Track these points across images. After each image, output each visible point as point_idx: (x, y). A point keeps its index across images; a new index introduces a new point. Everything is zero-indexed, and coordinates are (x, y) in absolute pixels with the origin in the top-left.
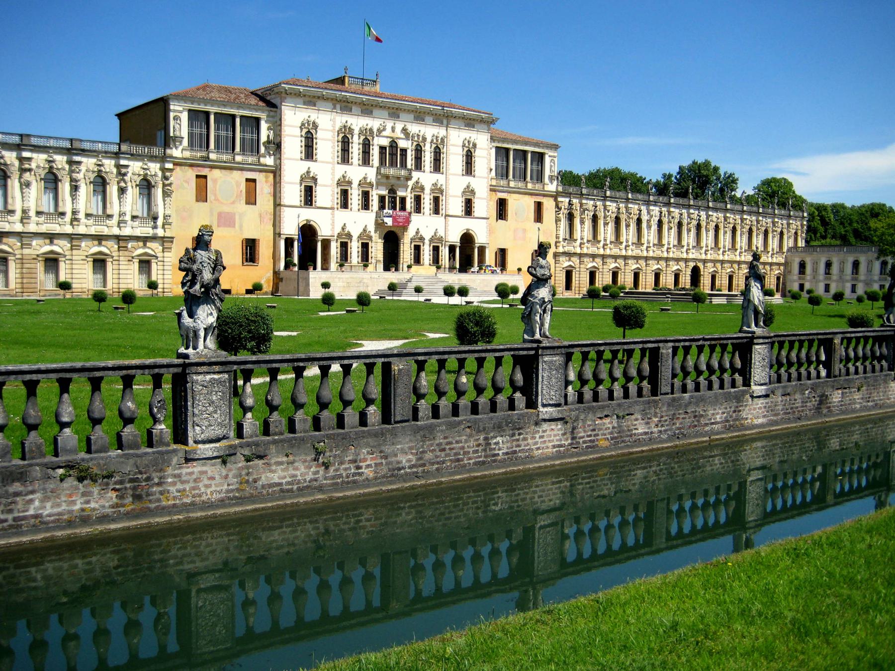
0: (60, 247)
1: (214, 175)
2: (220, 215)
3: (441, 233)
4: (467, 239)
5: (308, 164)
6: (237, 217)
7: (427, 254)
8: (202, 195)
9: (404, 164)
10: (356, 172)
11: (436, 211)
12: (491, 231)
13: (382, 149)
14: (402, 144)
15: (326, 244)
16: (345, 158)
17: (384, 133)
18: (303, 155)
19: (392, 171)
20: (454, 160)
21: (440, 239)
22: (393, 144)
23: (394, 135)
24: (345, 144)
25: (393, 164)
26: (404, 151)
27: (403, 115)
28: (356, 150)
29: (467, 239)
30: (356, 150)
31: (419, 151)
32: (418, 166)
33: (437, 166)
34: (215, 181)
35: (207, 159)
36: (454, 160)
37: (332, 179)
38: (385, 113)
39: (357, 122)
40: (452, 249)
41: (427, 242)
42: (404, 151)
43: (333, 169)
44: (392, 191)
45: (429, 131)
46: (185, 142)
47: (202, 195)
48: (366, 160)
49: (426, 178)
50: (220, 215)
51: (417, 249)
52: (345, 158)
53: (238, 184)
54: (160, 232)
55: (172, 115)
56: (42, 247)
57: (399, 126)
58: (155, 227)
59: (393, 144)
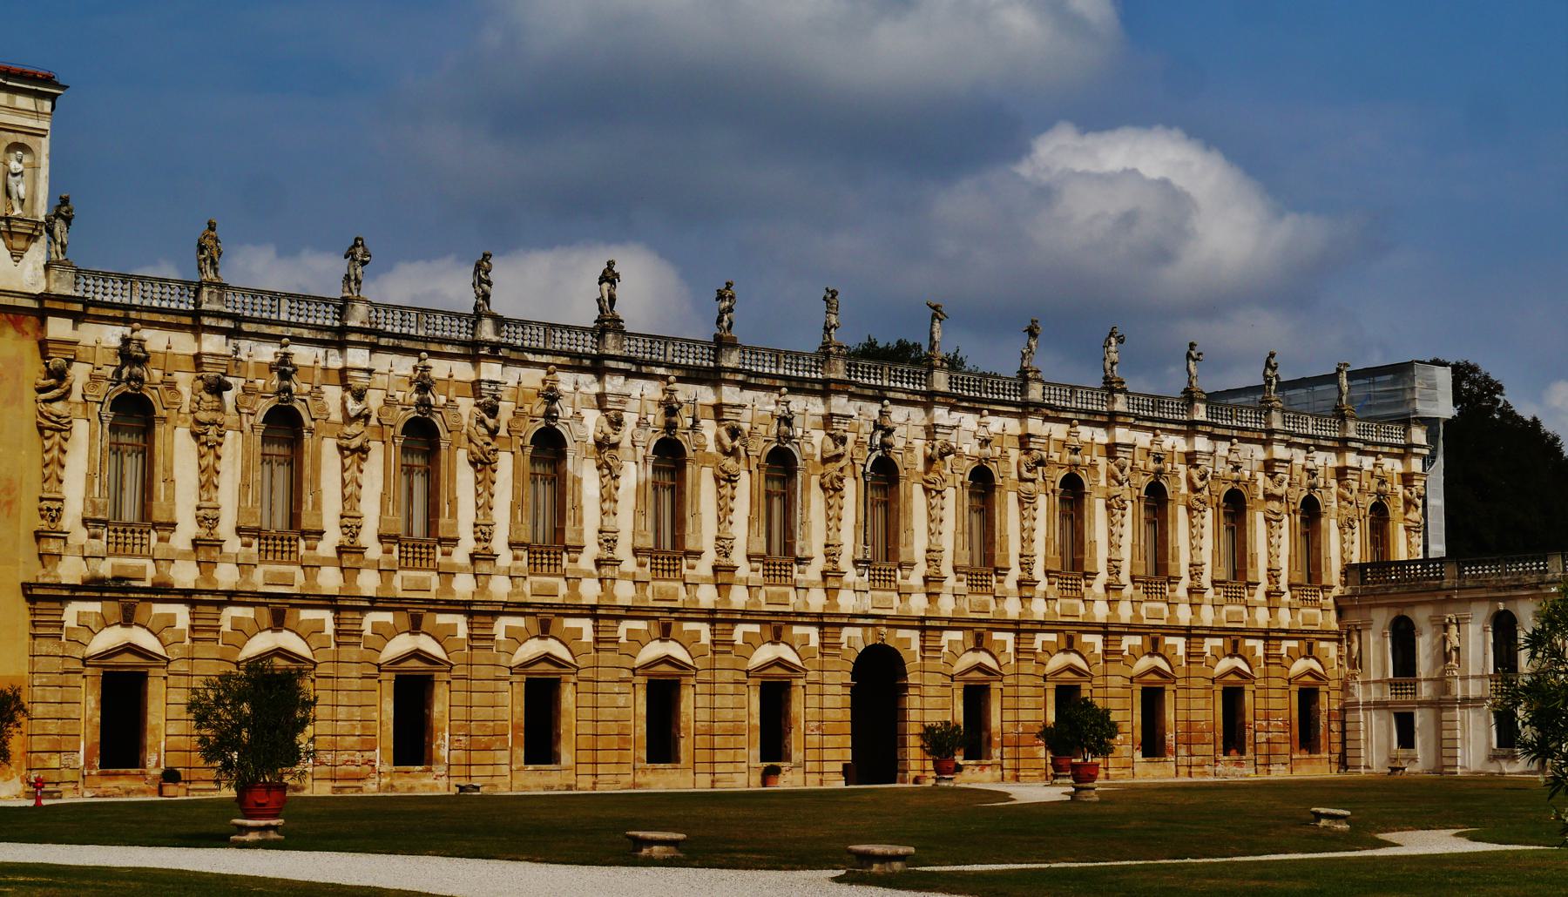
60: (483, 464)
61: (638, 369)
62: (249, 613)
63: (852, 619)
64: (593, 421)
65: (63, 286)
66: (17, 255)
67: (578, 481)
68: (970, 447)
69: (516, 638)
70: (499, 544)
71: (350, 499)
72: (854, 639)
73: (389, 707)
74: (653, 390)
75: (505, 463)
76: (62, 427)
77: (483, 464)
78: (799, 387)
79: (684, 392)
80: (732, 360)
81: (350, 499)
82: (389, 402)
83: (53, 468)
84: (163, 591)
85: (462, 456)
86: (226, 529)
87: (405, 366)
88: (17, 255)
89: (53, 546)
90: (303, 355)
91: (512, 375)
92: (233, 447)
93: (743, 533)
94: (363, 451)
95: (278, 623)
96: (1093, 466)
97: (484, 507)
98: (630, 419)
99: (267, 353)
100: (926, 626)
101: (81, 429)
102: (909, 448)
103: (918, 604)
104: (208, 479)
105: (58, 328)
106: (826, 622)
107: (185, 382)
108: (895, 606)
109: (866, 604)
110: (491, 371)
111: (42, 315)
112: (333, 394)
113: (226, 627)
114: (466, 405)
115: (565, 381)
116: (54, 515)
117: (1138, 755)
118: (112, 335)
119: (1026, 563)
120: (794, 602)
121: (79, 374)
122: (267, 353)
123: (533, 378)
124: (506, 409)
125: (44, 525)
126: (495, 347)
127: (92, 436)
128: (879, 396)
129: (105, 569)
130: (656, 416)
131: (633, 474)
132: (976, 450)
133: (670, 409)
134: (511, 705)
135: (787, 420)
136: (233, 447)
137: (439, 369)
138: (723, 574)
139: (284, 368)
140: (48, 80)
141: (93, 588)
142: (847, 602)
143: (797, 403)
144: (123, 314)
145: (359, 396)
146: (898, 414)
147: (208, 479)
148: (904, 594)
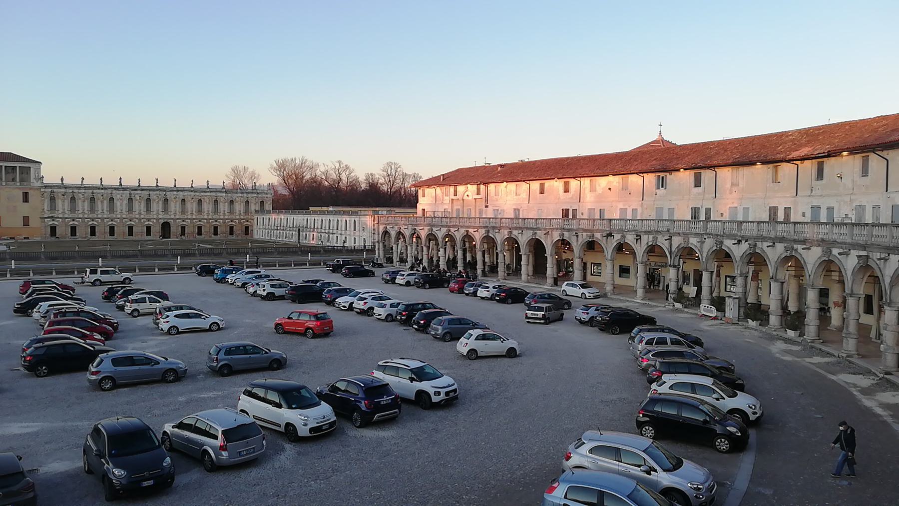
60: (102, 202)
62: (69, 220)
66: (37, 182)
67: (116, 203)
68: (182, 197)
69: (108, 222)
71: (83, 206)
72: (162, 221)
73: (89, 230)
75: (105, 201)
76: (44, 200)
77: (102, 202)
79: (132, 192)
81: (83, 206)
83: (43, 204)
84: (58, 218)
87: (91, 191)
88: (37, 182)
89: (43, 213)
90: (75, 191)
91: (106, 191)
92: (66, 201)
93: (161, 209)
97: (102, 207)
100: (175, 220)
101: (46, 200)
102: (171, 197)
103: (173, 217)
104: (63, 205)
105: (42, 190)
106: (157, 219)
108: (169, 217)
109: (164, 217)
110: (103, 191)
113: (66, 221)
118: (50, 190)
119: (208, 211)
120: (152, 217)
121: (45, 194)
122: (71, 191)
124: (105, 195)
125: (42, 211)
127: (48, 201)
129: (50, 215)
130: (128, 195)
131: (126, 202)
133: (130, 194)
134: (108, 229)
135: (149, 195)
136: (66, 201)
137: (95, 191)
138: (224, 214)
140: (40, 162)
141: (48, 217)
142: (160, 216)
143: (151, 192)
145: (83, 195)
146: (168, 193)
148: (170, 215)
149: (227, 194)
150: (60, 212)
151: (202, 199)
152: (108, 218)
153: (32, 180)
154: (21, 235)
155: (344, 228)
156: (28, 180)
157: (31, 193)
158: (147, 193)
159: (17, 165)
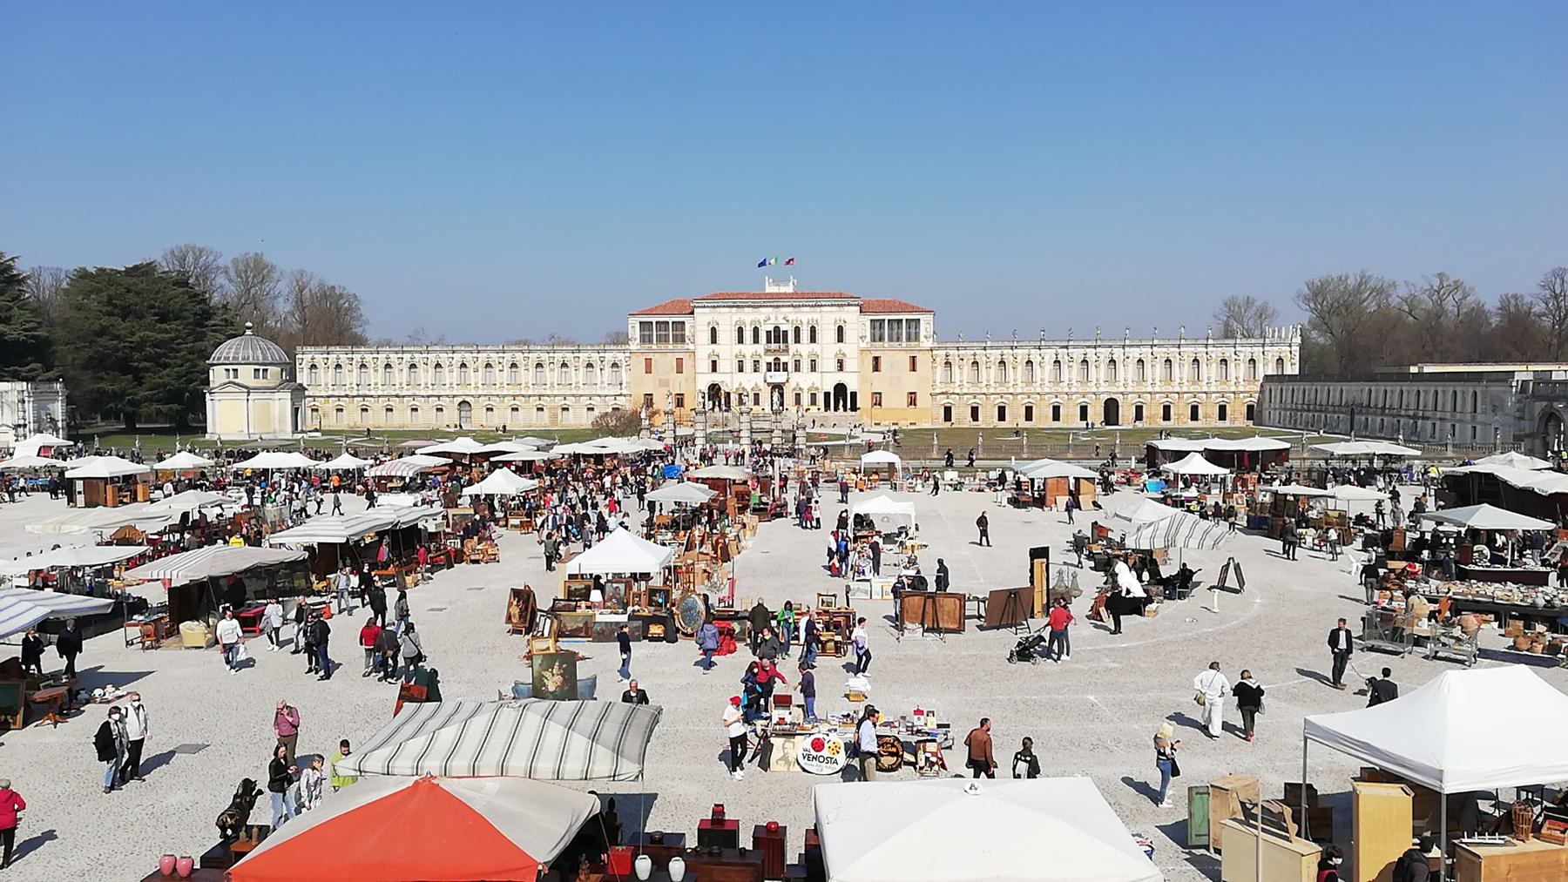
0: (570, 402)
1: (655, 358)
2: (660, 380)
3: (818, 384)
4: (840, 389)
5: (714, 346)
6: (671, 382)
7: (806, 399)
8: (648, 371)
9: (786, 341)
10: (749, 348)
11: (813, 369)
12: (863, 380)
13: (768, 333)
14: (783, 328)
15: (728, 395)
16: (741, 340)
17: (769, 322)
18: (710, 342)
19: (773, 346)
20: (827, 334)
21: (817, 389)
22: (777, 329)
23: (777, 322)
24: (740, 331)
25: (777, 341)
26: (785, 332)
27: (783, 309)
28: (748, 335)
29: (840, 389)
30: (748, 335)
31: (797, 330)
32: (797, 340)
33: (813, 339)
34: (656, 361)
35: (650, 348)
36: (827, 334)
37: (731, 355)
38: (771, 309)
39: (748, 317)
40: (827, 395)
41: (806, 390)
42: (785, 332)
43: (732, 348)
44: (777, 359)
45: (804, 317)
46: (638, 341)
47: (648, 371)
48: (756, 340)
49: (804, 348)
50: (660, 380)
51: (798, 395)
52: (741, 340)
53: (672, 361)
54: (624, 392)
55: (630, 326)
56: (560, 402)
57: (780, 317)
58: (621, 389)
59: (777, 329)
61: (1049, 347)
63: (1103, 393)
64: (1039, 358)
65: (936, 345)
70: (1019, 382)
72: (1106, 397)
74: (1054, 351)
75: (1020, 368)
78: (1089, 347)
79: (1060, 351)
80: (1071, 343)
82: (995, 359)
83: (934, 374)
85: (1011, 367)
86: (965, 383)
94: (990, 368)
95: (975, 398)
96: (1175, 357)
98: (1047, 358)
99: (972, 352)
103: (1122, 389)
104: (961, 374)
107: (957, 359)
108: (1116, 390)
111: (932, 350)
112: (984, 358)
114: (1012, 358)
115: (1033, 351)
116: (934, 382)
117: (1189, 420)
118: (944, 352)
121: (938, 359)
122: (972, 352)
123: (1026, 351)
126: (1016, 347)
128: (1111, 347)
129: (944, 390)
132: (1139, 356)
137: (1005, 352)
139: (975, 355)
142: (1101, 390)
143: (1088, 350)
144: (946, 348)
147: (961, 374)
148: (1118, 387)
149: (1215, 349)
150: (957, 385)
151: (1171, 359)
152: (1023, 394)
153: (922, 338)
154: (906, 420)
155: (1449, 407)
156: (917, 339)
157: (919, 357)
158: (1082, 351)
159: (904, 317)
